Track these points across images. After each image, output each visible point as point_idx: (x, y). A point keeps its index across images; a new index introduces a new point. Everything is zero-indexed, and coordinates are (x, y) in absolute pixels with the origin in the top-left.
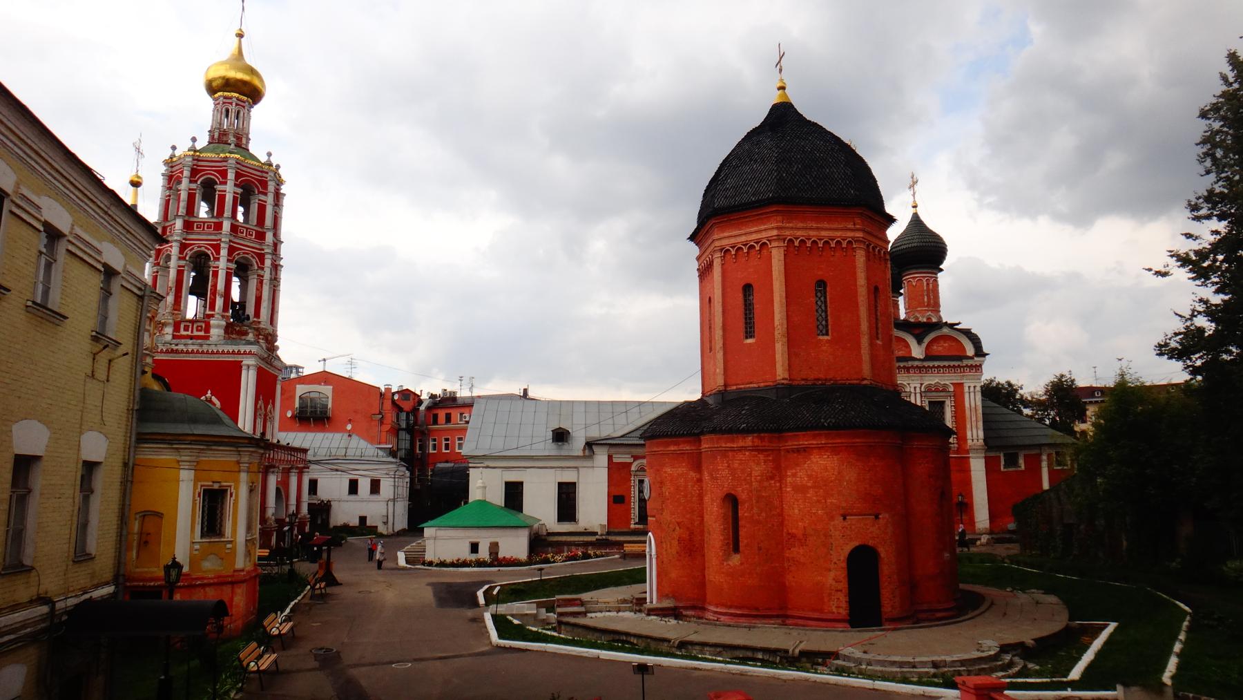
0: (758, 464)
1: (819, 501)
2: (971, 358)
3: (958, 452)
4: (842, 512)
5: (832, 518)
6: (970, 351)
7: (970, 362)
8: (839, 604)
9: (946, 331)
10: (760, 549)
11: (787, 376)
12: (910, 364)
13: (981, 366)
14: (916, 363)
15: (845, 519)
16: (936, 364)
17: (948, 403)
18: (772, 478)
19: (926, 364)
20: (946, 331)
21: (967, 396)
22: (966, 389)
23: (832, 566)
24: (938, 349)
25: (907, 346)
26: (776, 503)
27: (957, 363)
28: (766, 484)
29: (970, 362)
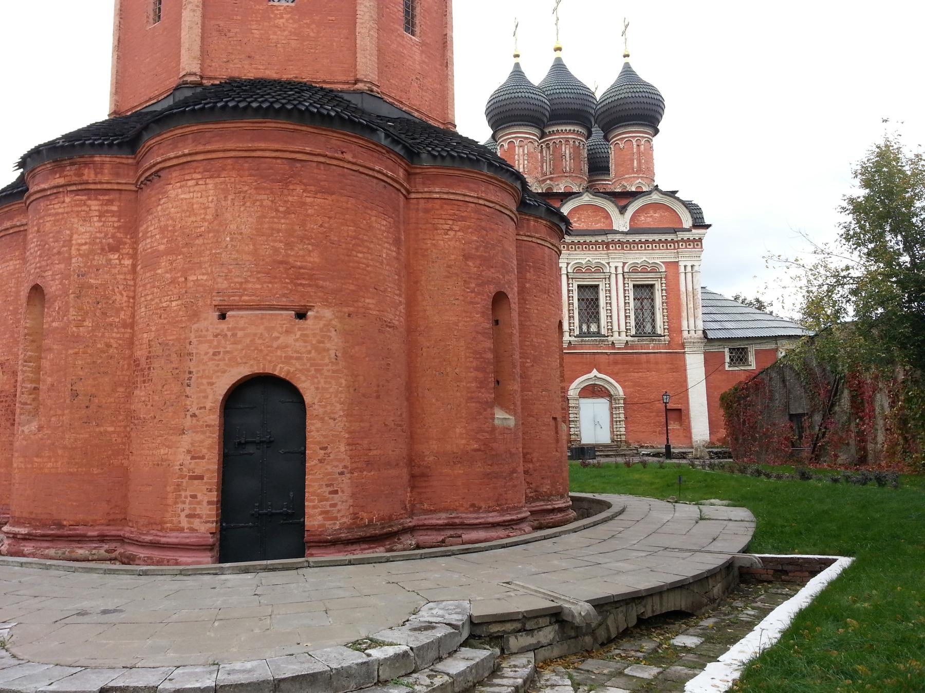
0: (86, 219)
1: (173, 281)
2: (689, 230)
3: (669, 345)
4: (217, 300)
5: (195, 316)
6: (687, 222)
7: (686, 236)
8: (196, 510)
9: (655, 197)
10: (75, 394)
11: (196, 69)
12: (610, 237)
13: (700, 240)
14: (617, 237)
15: (223, 317)
16: (643, 238)
17: (658, 286)
18: (114, 249)
19: (630, 238)
20: (655, 197)
21: (682, 276)
22: (682, 269)
23: (188, 422)
24: (646, 220)
25: (608, 216)
26: (121, 299)
27: (669, 237)
28: (100, 260)
29: (686, 236)
